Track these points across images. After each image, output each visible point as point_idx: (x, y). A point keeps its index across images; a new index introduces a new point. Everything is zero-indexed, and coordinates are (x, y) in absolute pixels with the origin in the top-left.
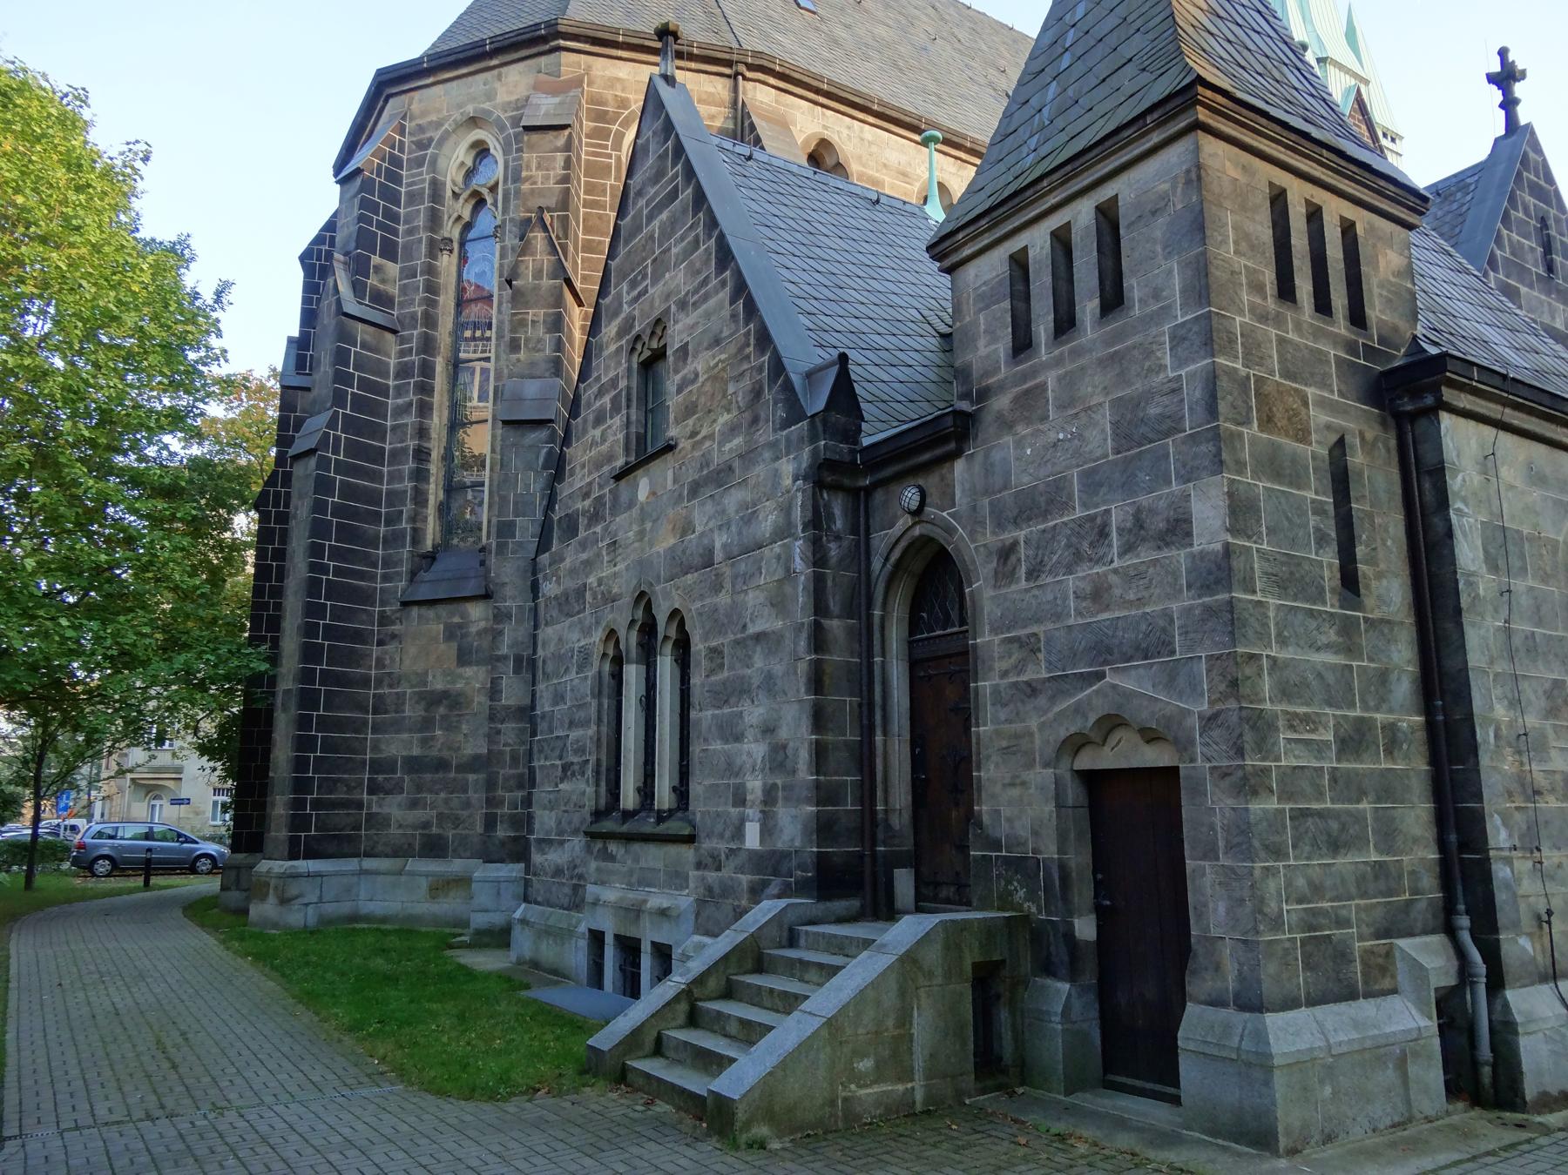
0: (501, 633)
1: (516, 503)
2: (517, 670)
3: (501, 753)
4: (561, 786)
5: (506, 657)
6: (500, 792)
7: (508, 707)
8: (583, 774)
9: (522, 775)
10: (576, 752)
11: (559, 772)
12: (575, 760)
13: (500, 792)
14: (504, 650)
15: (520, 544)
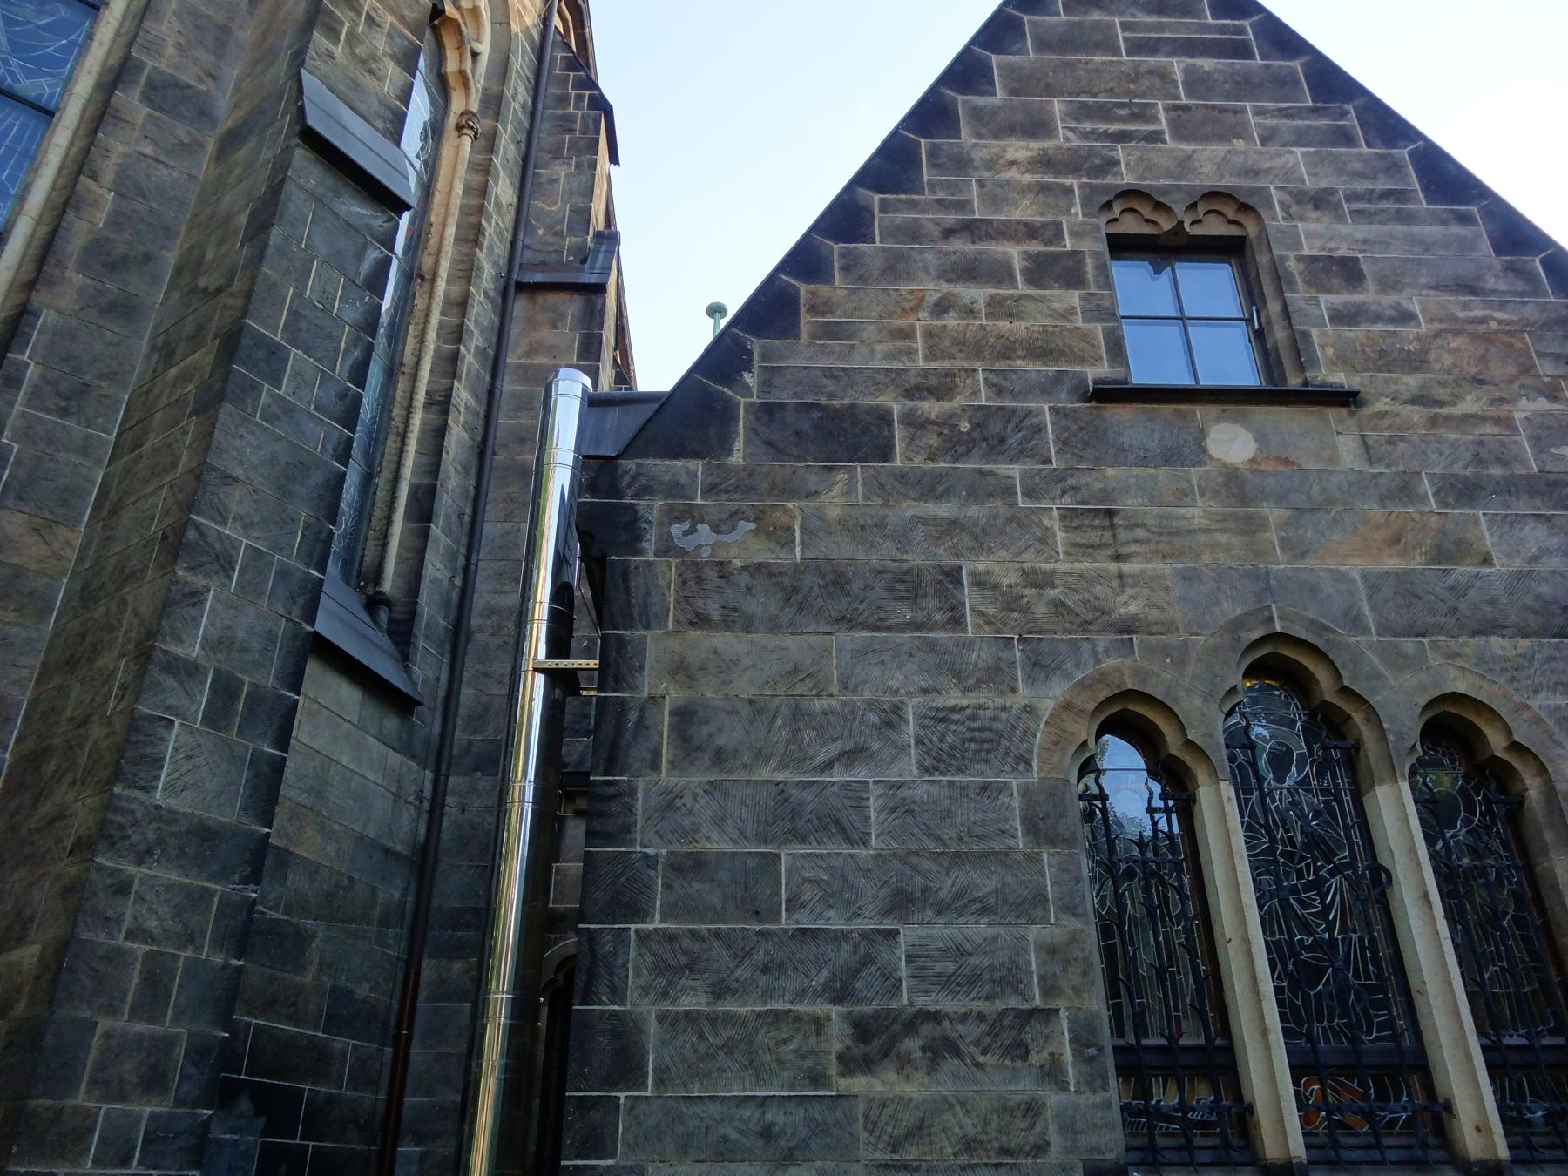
0: (195, 598)
1: (294, 315)
2: (216, 717)
3: (117, 958)
4: (858, 1084)
5: (188, 671)
6: (81, 1099)
7: (172, 817)
8: (1020, 1050)
9: (168, 1042)
10: (947, 983)
11: (838, 1037)
12: (949, 1004)
13: (81, 1099)
14: (193, 650)
15: (288, 409)
